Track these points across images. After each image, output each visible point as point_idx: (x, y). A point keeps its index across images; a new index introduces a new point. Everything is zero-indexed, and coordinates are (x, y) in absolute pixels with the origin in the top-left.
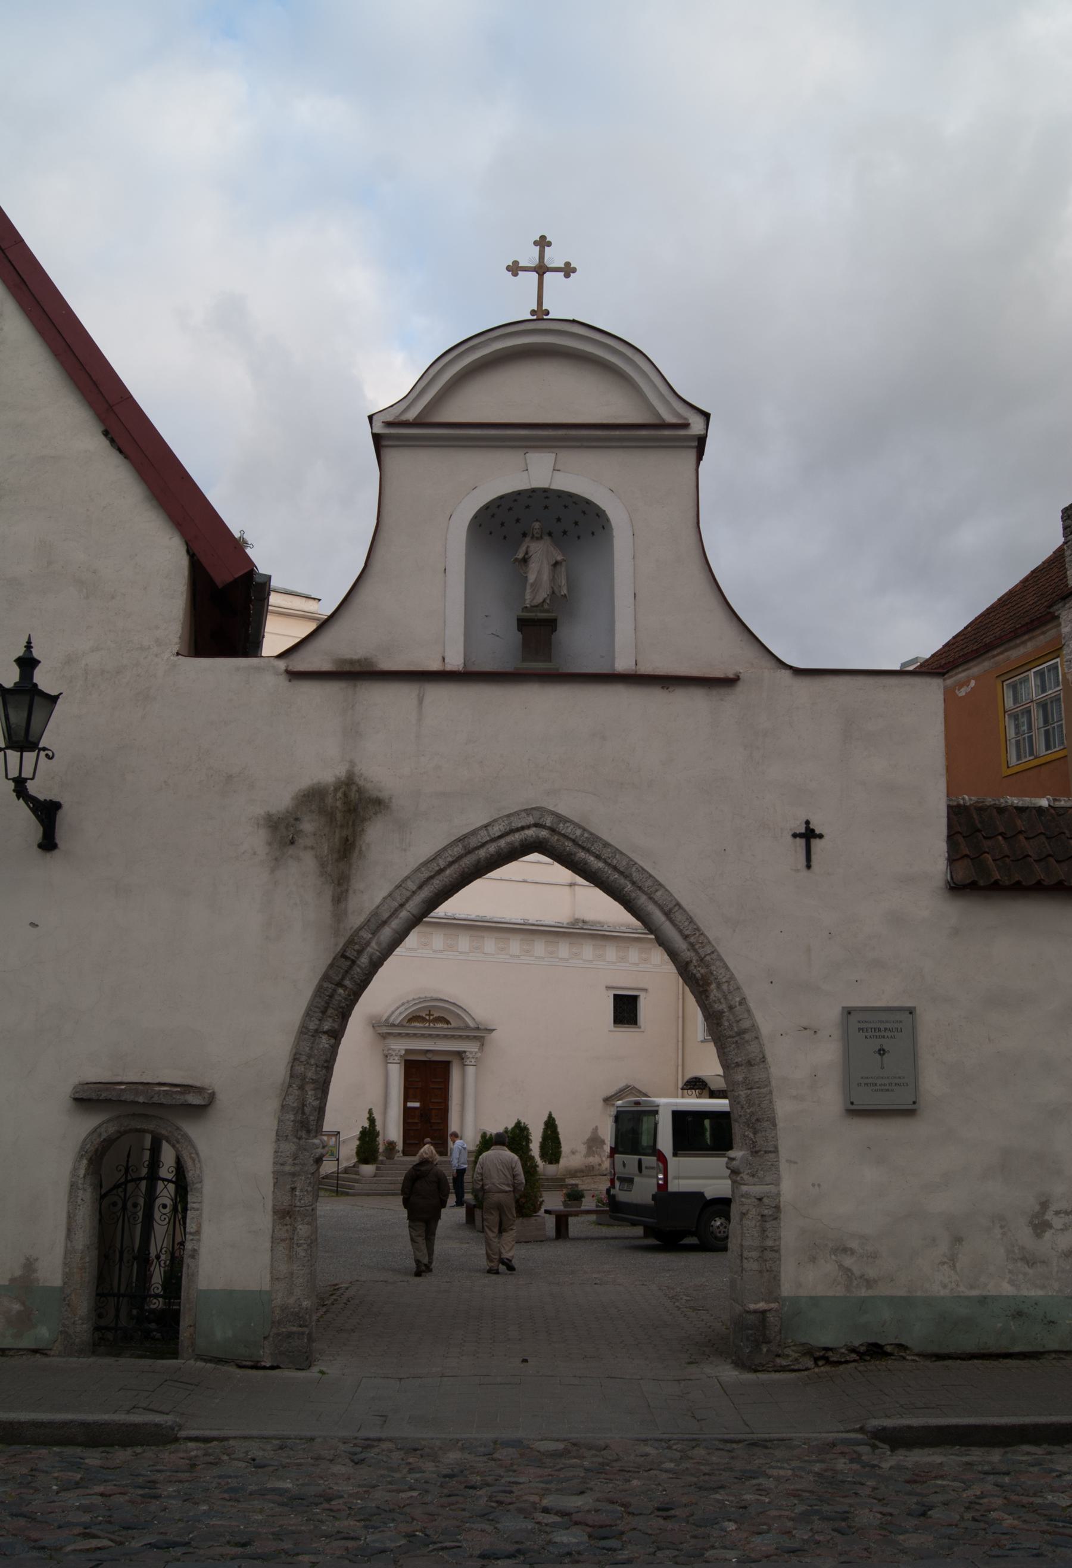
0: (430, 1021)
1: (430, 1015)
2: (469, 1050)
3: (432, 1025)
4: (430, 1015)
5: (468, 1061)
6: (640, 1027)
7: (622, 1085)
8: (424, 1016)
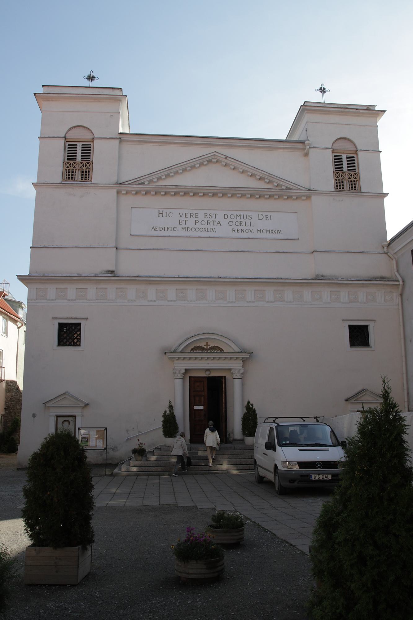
0: (207, 350)
1: (207, 345)
2: (235, 368)
3: (208, 351)
4: (207, 345)
5: (235, 375)
6: (371, 347)
7: (359, 389)
8: (203, 346)
